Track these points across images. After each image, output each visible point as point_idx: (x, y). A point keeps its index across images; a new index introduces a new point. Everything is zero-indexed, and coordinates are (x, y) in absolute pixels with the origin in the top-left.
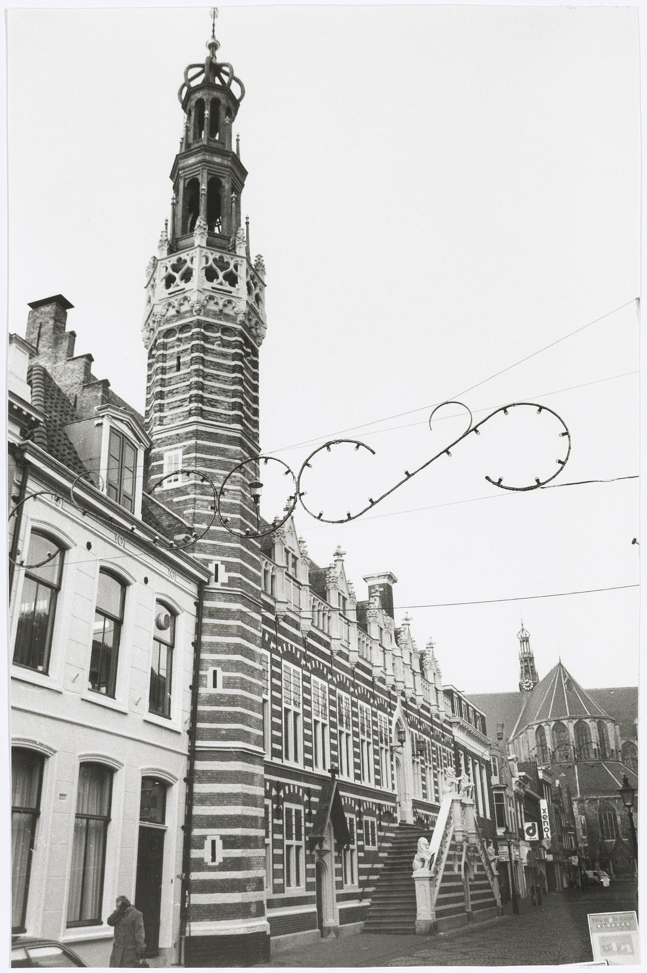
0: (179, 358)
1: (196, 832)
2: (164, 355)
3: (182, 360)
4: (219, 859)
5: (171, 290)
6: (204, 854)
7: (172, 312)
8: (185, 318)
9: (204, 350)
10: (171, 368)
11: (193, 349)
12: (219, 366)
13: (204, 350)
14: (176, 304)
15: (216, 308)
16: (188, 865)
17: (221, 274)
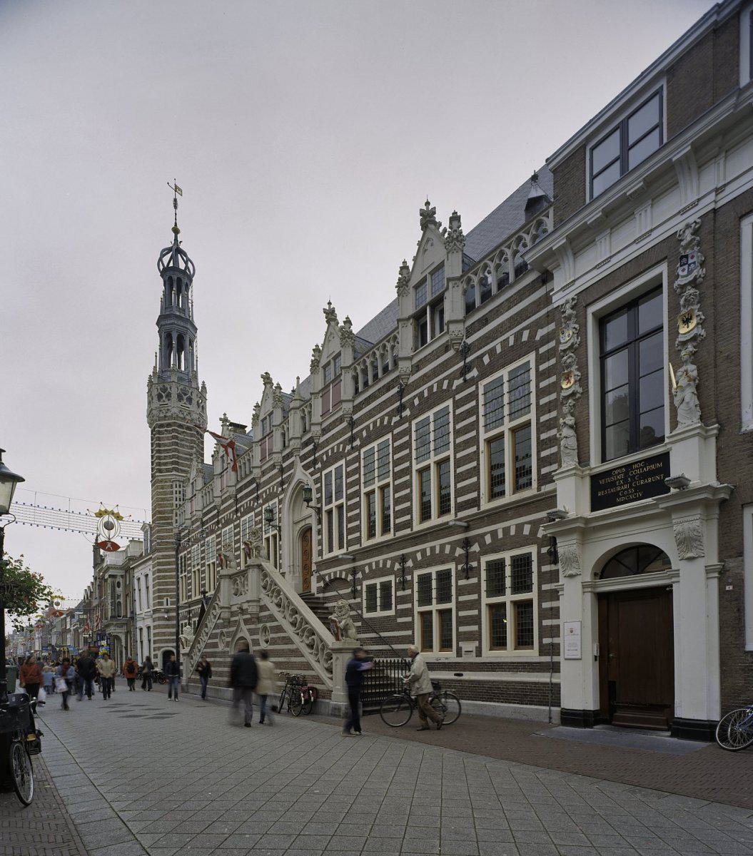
2: (159, 437)
7: (162, 415)
15: (182, 416)
17: (185, 397)
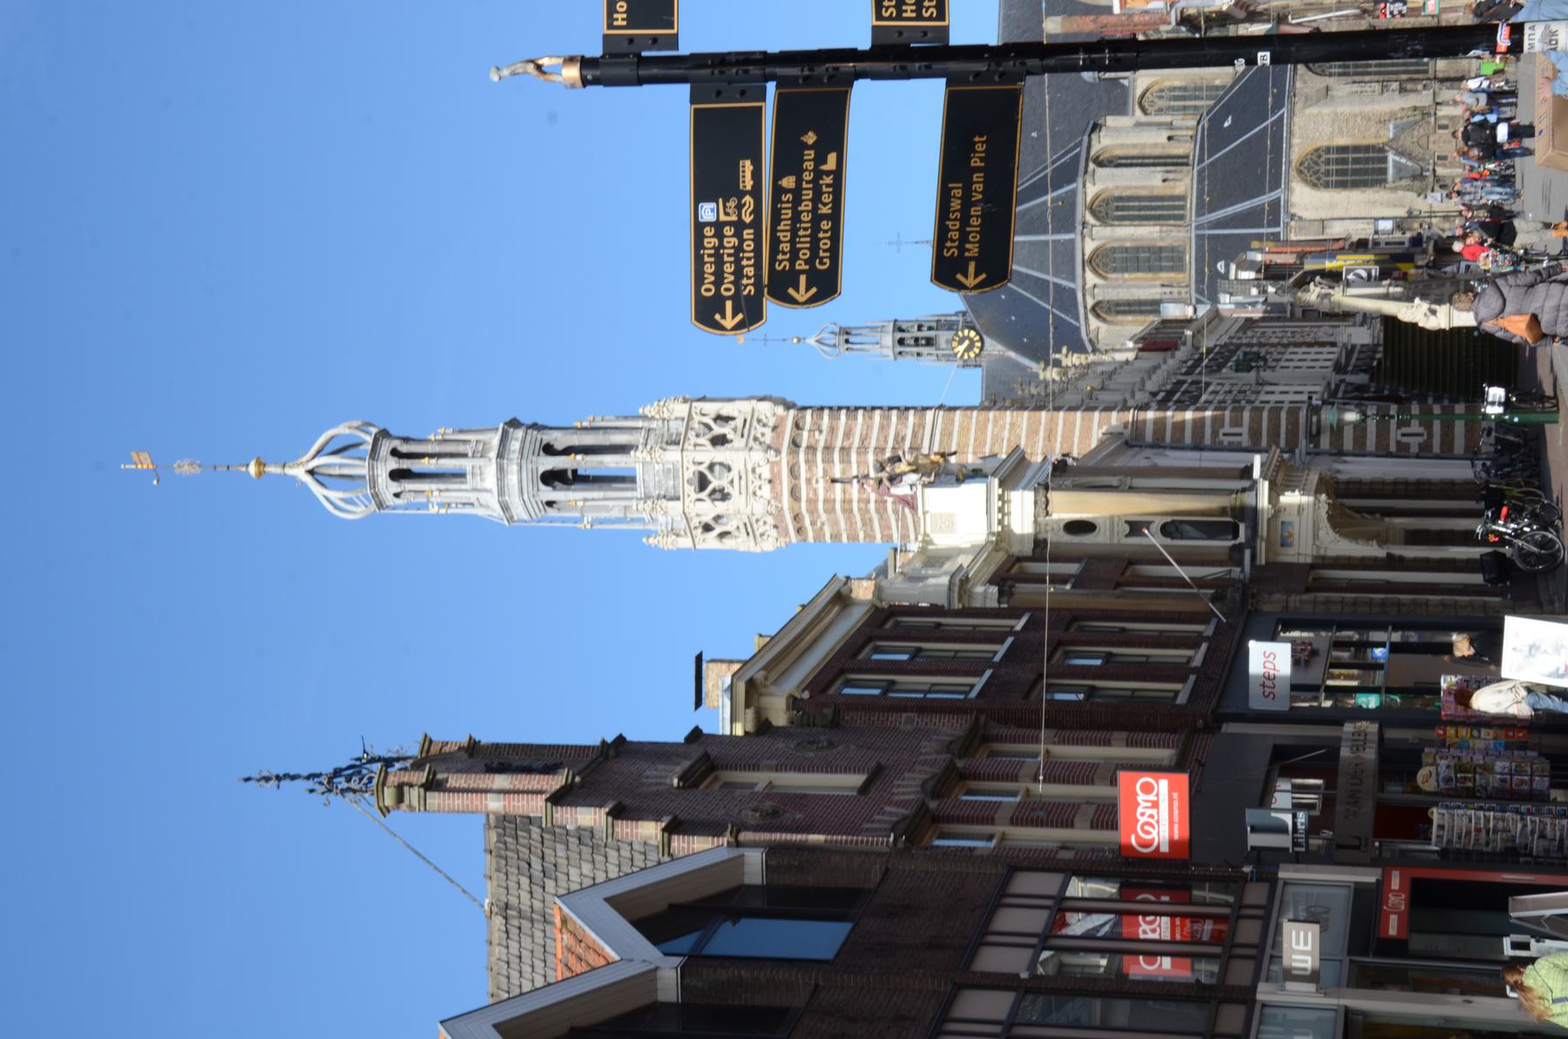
0: (834, 481)
1: (1393, 448)
3: (838, 475)
4: (1421, 430)
5: (734, 492)
6: (1414, 443)
8: (779, 472)
9: (828, 448)
10: (844, 491)
11: (828, 460)
12: (847, 435)
13: (828, 448)
14: (757, 483)
16: (1424, 452)
